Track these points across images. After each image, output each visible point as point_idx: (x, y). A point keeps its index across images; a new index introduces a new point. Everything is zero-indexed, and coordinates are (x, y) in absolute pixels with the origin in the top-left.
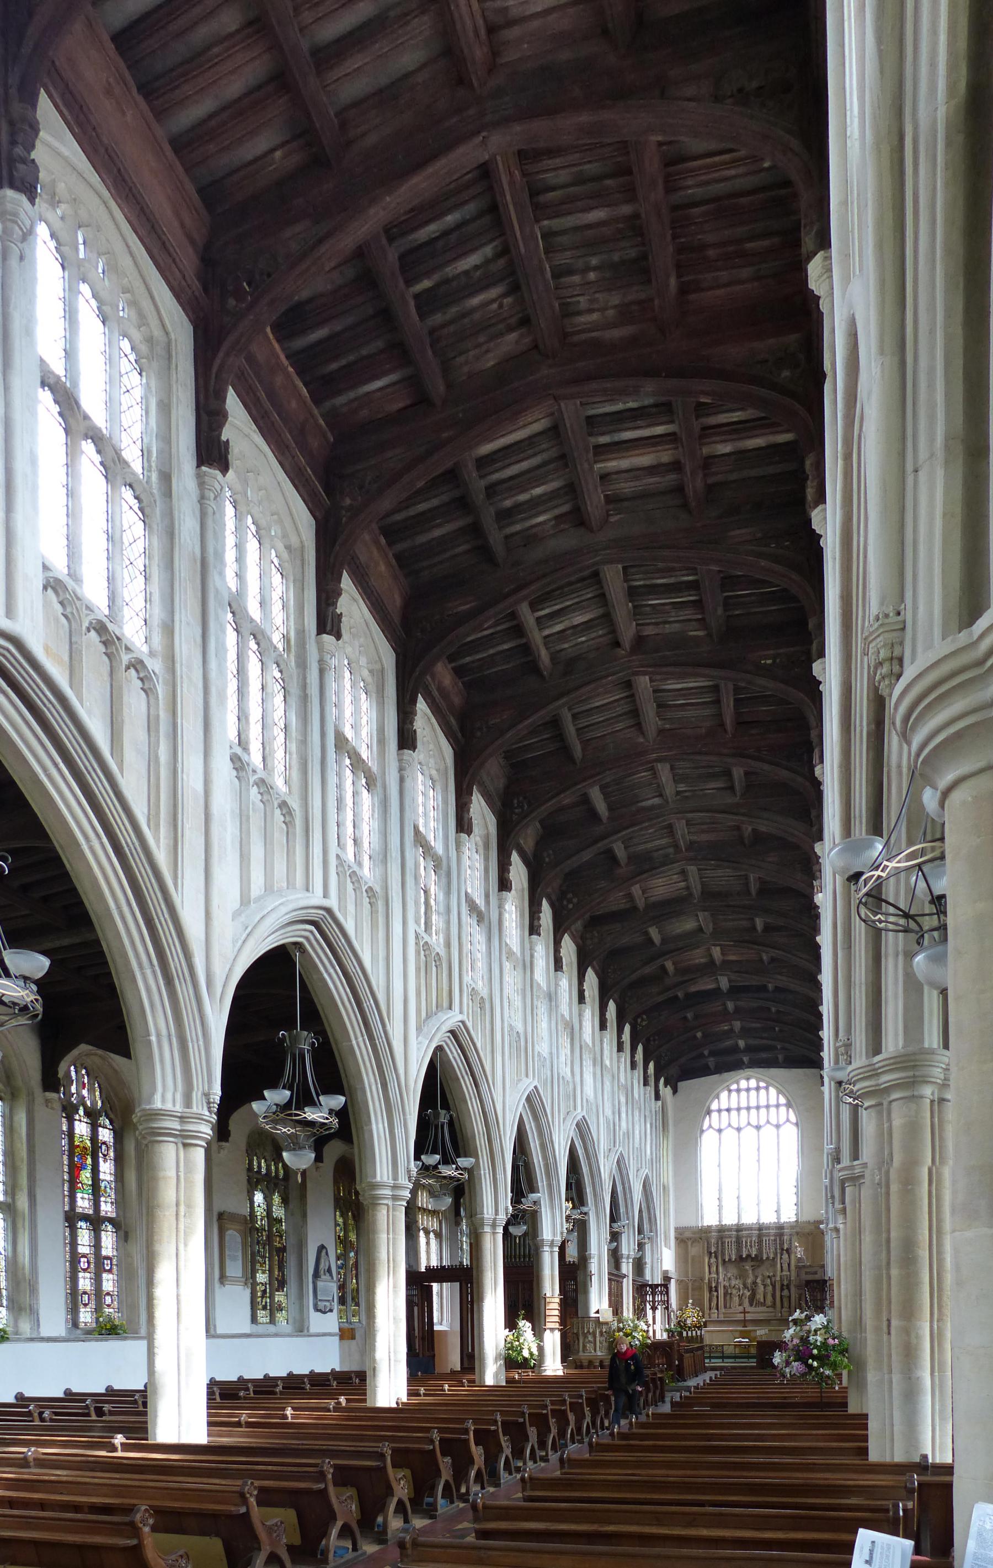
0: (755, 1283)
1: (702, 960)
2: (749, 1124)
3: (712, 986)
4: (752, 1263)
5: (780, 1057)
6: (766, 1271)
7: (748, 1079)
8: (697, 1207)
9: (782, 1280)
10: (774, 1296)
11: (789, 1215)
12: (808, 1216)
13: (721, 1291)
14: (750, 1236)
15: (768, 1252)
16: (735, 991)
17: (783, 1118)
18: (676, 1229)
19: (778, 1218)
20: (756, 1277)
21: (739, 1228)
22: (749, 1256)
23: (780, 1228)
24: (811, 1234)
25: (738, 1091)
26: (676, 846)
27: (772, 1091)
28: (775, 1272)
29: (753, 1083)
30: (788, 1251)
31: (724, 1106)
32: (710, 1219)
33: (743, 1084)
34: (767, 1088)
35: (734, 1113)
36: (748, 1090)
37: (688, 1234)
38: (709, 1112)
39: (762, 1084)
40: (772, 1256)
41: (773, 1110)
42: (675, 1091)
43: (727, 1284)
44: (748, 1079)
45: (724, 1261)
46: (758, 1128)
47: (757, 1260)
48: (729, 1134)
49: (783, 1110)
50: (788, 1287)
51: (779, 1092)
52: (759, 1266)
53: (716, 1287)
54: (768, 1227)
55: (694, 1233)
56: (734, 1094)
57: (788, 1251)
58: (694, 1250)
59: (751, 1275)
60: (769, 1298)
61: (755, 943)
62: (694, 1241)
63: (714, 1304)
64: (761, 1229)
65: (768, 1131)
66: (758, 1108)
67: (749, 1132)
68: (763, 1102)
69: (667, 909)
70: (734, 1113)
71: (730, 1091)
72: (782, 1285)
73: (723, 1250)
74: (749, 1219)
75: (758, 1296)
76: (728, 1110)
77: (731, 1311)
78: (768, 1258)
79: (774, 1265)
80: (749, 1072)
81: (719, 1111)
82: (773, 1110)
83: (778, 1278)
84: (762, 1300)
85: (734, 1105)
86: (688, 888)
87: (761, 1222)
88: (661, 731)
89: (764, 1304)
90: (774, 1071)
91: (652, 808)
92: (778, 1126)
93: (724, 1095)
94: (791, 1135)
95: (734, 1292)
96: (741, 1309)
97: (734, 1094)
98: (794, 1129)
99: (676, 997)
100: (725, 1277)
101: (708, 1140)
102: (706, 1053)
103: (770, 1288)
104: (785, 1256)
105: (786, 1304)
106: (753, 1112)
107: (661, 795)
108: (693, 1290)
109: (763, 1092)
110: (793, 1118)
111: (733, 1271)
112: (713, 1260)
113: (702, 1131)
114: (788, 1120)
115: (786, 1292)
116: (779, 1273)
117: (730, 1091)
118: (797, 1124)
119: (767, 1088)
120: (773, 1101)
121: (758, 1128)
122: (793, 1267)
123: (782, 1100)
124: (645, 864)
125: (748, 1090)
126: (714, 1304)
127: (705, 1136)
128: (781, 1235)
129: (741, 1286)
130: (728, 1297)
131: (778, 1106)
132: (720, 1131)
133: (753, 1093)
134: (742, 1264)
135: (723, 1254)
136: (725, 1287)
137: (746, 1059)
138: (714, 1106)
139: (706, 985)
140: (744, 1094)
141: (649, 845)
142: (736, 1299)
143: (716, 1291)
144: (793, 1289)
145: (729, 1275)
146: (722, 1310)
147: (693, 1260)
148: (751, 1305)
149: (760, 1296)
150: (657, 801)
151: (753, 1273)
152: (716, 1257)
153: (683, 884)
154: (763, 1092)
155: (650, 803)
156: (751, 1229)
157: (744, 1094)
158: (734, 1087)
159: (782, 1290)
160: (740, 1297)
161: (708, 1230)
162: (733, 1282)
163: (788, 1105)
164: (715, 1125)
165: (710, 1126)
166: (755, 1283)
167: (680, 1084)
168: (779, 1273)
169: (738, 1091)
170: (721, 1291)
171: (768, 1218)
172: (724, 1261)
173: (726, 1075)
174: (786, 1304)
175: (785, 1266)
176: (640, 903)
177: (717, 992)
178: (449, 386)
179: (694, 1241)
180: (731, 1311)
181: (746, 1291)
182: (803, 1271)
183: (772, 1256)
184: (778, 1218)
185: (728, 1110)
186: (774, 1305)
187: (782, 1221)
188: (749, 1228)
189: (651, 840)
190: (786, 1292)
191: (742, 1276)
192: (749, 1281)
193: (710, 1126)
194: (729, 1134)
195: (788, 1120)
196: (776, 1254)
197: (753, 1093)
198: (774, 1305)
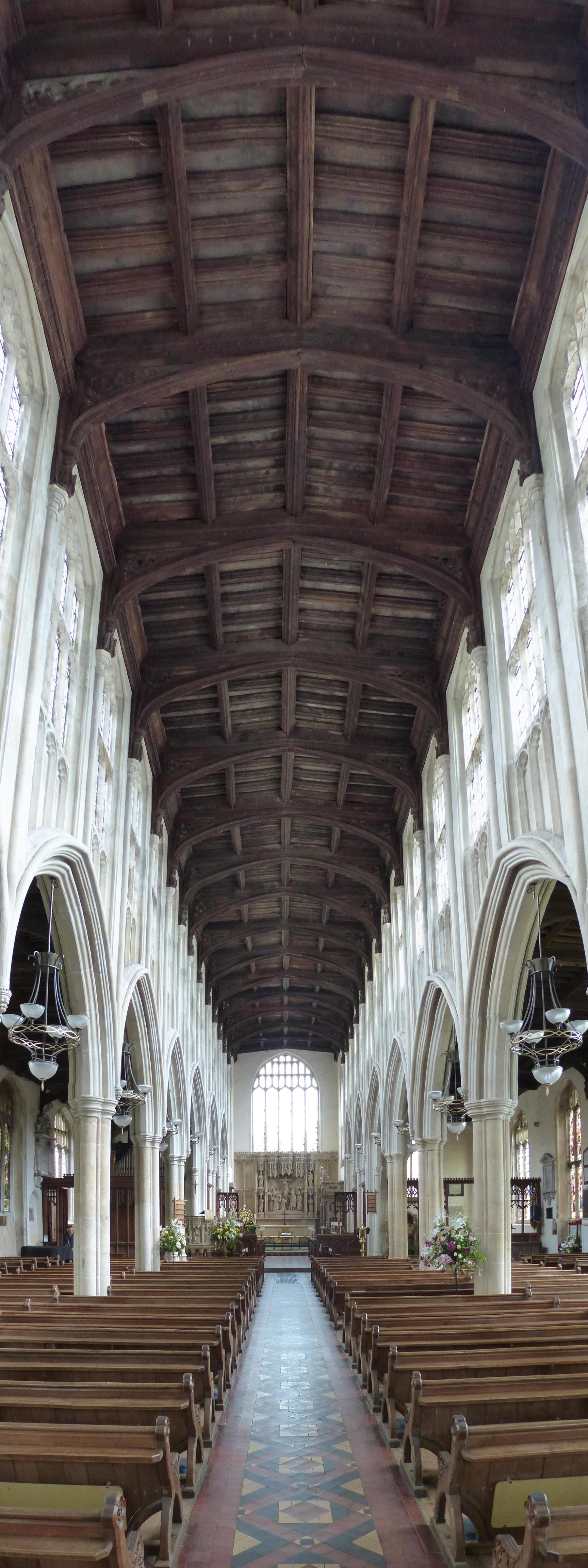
0: (290, 1194)
1: (275, 966)
2: (285, 1086)
3: (278, 985)
5: (309, 1042)
6: (296, 1185)
7: (285, 1056)
8: (250, 1139)
9: (308, 1193)
10: (303, 1203)
11: (313, 1147)
12: (327, 1148)
14: (287, 1160)
15: (299, 1172)
16: (292, 990)
17: (308, 1084)
18: (235, 1154)
19: (306, 1148)
20: (291, 1190)
21: (279, 1155)
22: (286, 1174)
23: (308, 1156)
24: (330, 1160)
25: (279, 1063)
26: (280, 881)
27: (302, 1065)
28: (304, 1186)
29: (288, 1058)
30: (312, 1172)
31: (269, 1072)
32: (258, 1147)
33: (282, 1058)
34: (298, 1062)
35: (275, 1078)
36: (285, 1063)
37: (243, 1158)
38: (258, 1076)
39: (295, 1060)
40: (301, 1175)
41: (302, 1078)
42: (236, 1060)
44: (285, 1056)
45: (269, 1178)
46: (292, 1089)
47: (291, 1177)
48: (272, 1092)
49: (308, 1078)
50: (313, 1197)
51: (306, 1066)
53: (263, 1196)
54: (299, 1155)
55: (247, 1157)
56: (276, 1065)
57: (312, 1172)
58: (247, 1169)
60: (300, 1204)
61: (315, 957)
62: (248, 1162)
63: (261, 1208)
64: (294, 1155)
65: (298, 1092)
66: (292, 1075)
67: (285, 1092)
68: (295, 1072)
69: (263, 925)
70: (275, 1078)
71: (273, 1063)
72: (309, 1196)
73: (268, 1168)
74: (285, 1149)
76: (272, 1076)
77: (274, 1213)
79: (303, 1182)
80: (286, 1051)
81: (266, 1076)
82: (302, 1078)
83: (306, 1191)
85: (275, 1072)
86: (280, 913)
87: (294, 1151)
88: (293, 797)
89: (296, 1209)
90: (303, 1052)
91: (274, 850)
92: (305, 1089)
93: (269, 1065)
94: (313, 1095)
95: (276, 1199)
96: (280, 1212)
97: (276, 1065)
98: (316, 1091)
99: (252, 989)
100: (271, 1189)
101: (257, 1096)
102: (261, 1034)
103: (300, 1198)
104: (311, 1175)
105: (311, 1209)
106: (289, 1078)
107: (280, 843)
109: (295, 1065)
110: (315, 1085)
111: (274, 1185)
112: (261, 1177)
113: (254, 1089)
114: (312, 1085)
115: (311, 1201)
116: (306, 1187)
117: (273, 1063)
118: (317, 1088)
119: (298, 1062)
120: (302, 1072)
121: (292, 1089)
123: (308, 1072)
124: (257, 891)
125: (285, 1063)
126: (261, 1208)
127: (255, 1093)
128: (308, 1161)
131: (305, 1075)
132: (266, 1089)
133: (289, 1065)
135: (268, 1173)
137: (285, 1042)
138: (262, 1072)
139: (274, 984)
140: (282, 1065)
141: (262, 878)
142: (277, 1205)
143: (263, 1198)
144: (316, 1198)
148: (287, 1209)
149: (293, 1203)
150: (277, 846)
152: (263, 1175)
153: (277, 909)
154: (295, 1065)
155: (270, 847)
156: (287, 1156)
157: (282, 1065)
158: (276, 1060)
159: (308, 1199)
160: (280, 1204)
161: (257, 1155)
162: (275, 1193)
163: (312, 1075)
164: (263, 1085)
165: (259, 1086)
166: (290, 1194)
167: (239, 1055)
168: (306, 1187)
169: (279, 1063)
171: (299, 1149)
172: (269, 1178)
173: (271, 1052)
174: (311, 1209)
175: (311, 1183)
176: (246, 918)
177: (279, 990)
178: (219, 514)
179: (248, 1162)
182: (328, 1186)
183: (301, 1175)
184: (306, 1148)
185: (272, 1076)
186: (303, 1209)
187: (308, 1151)
188: (287, 1155)
189: (264, 874)
190: (311, 1201)
191: (281, 1188)
192: (286, 1192)
193: (259, 1086)
194: (272, 1092)
195: (312, 1085)
196: (304, 1173)
197: (289, 1065)
198: (303, 1209)
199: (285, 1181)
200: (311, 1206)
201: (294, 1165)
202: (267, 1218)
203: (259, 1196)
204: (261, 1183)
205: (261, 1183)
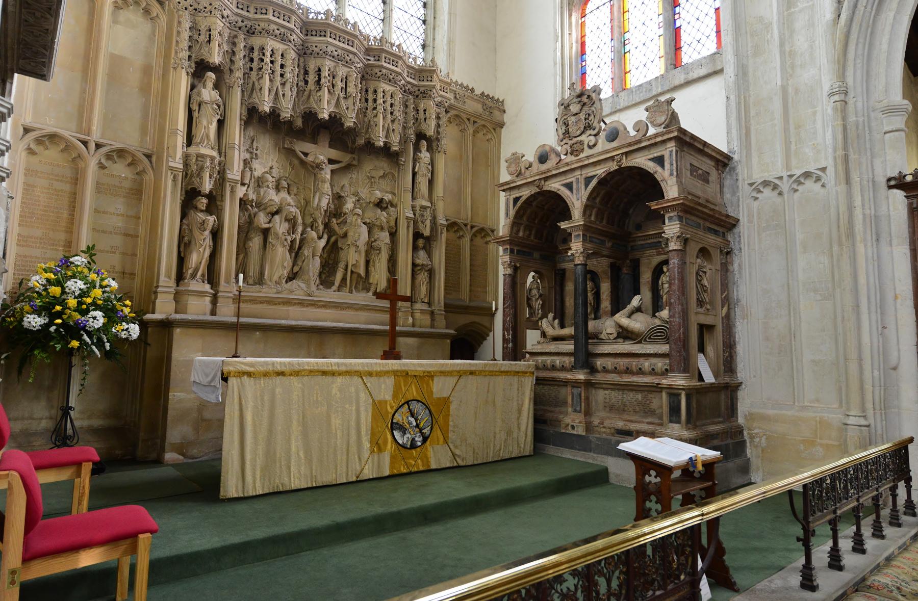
0: (336, 212)
4: (334, 154)
6: (364, 185)
13: (231, 217)
22: (335, 121)
43: (252, 196)
52: (348, 168)
59: (327, 187)
63: (198, 257)
77: (267, 292)
78: (387, 147)
84: (362, 272)
89: (363, 282)
95: (280, 226)
104: (425, 155)
108: (99, 188)
122: (439, 190)
126: (198, 257)
130: (255, 243)
134: (301, 147)
135: (250, 89)
136: (243, 203)
142: (280, 256)
145: (259, 169)
146: (228, 288)
147: (113, 78)
149: (353, 257)
160: (296, 251)
162: (274, 197)
166: (336, 212)
170: (231, 217)
175: (423, 186)
180: (267, 292)
199: (320, 153)
200: (423, 277)
201: (367, 95)
202: (226, 313)
203: (190, 196)
204: (208, 126)
205: (208, 126)
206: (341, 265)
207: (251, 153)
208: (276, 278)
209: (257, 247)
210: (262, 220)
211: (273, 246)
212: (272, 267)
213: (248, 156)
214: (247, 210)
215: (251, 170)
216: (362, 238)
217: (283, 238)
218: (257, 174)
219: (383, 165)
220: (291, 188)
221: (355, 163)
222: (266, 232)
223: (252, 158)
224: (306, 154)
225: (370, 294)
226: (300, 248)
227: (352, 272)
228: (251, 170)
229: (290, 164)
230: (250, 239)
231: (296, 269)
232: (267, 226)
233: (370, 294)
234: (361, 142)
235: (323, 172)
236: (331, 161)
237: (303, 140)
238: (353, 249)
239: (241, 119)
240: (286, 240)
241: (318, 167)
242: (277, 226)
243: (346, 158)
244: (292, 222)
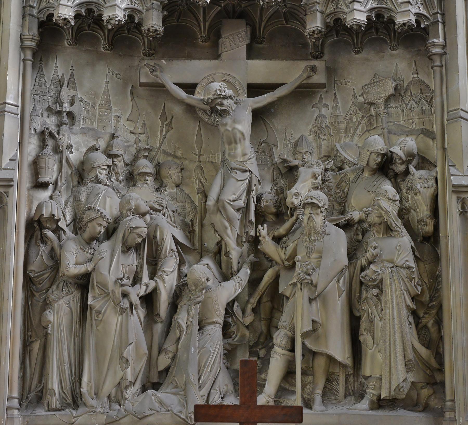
4: (260, 70)
20: (290, 172)
43: (57, 206)
52: (304, 93)
75: (299, 313)
84: (337, 346)
89: (350, 377)
95: (113, 265)
103: (400, 247)
129: (170, 233)
130: (61, 310)
134: (174, 73)
136: (35, 227)
142: (122, 331)
149: (314, 315)
151: (263, 147)
162: (107, 203)
181: (203, 270)
206: (280, 338)
207: (59, 113)
208: (109, 387)
209: (65, 321)
210: (73, 261)
211: (98, 312)
212: (99, 361)
213: (51, 122)
214: (44, 240)
215: (57, 150)
216: (327, 261)
217: (119, 291)
218: (74, 157)
219: (396, 64)
220: (165, 172)
221: (319, 78)
222: (84, 283)
223: (60, 125)
224: (190, 88)
225: (364, 404)
226: (174, 307)
227: (310, 355)
228: (57, 150)
229: (164, 116)
230: (47, 305)
231: (163, 361)
232: (81, 269)
233: (364, 404)
234: (315, 23)
235: (228, 120)
236: (254, 90)
237: (190, 57)
238: (302, 296)
239: (23, 48)
240: (125, 295)
241: (215, 109)
242: (103, 266)
243: (287, 72)
244: (150, 251)
